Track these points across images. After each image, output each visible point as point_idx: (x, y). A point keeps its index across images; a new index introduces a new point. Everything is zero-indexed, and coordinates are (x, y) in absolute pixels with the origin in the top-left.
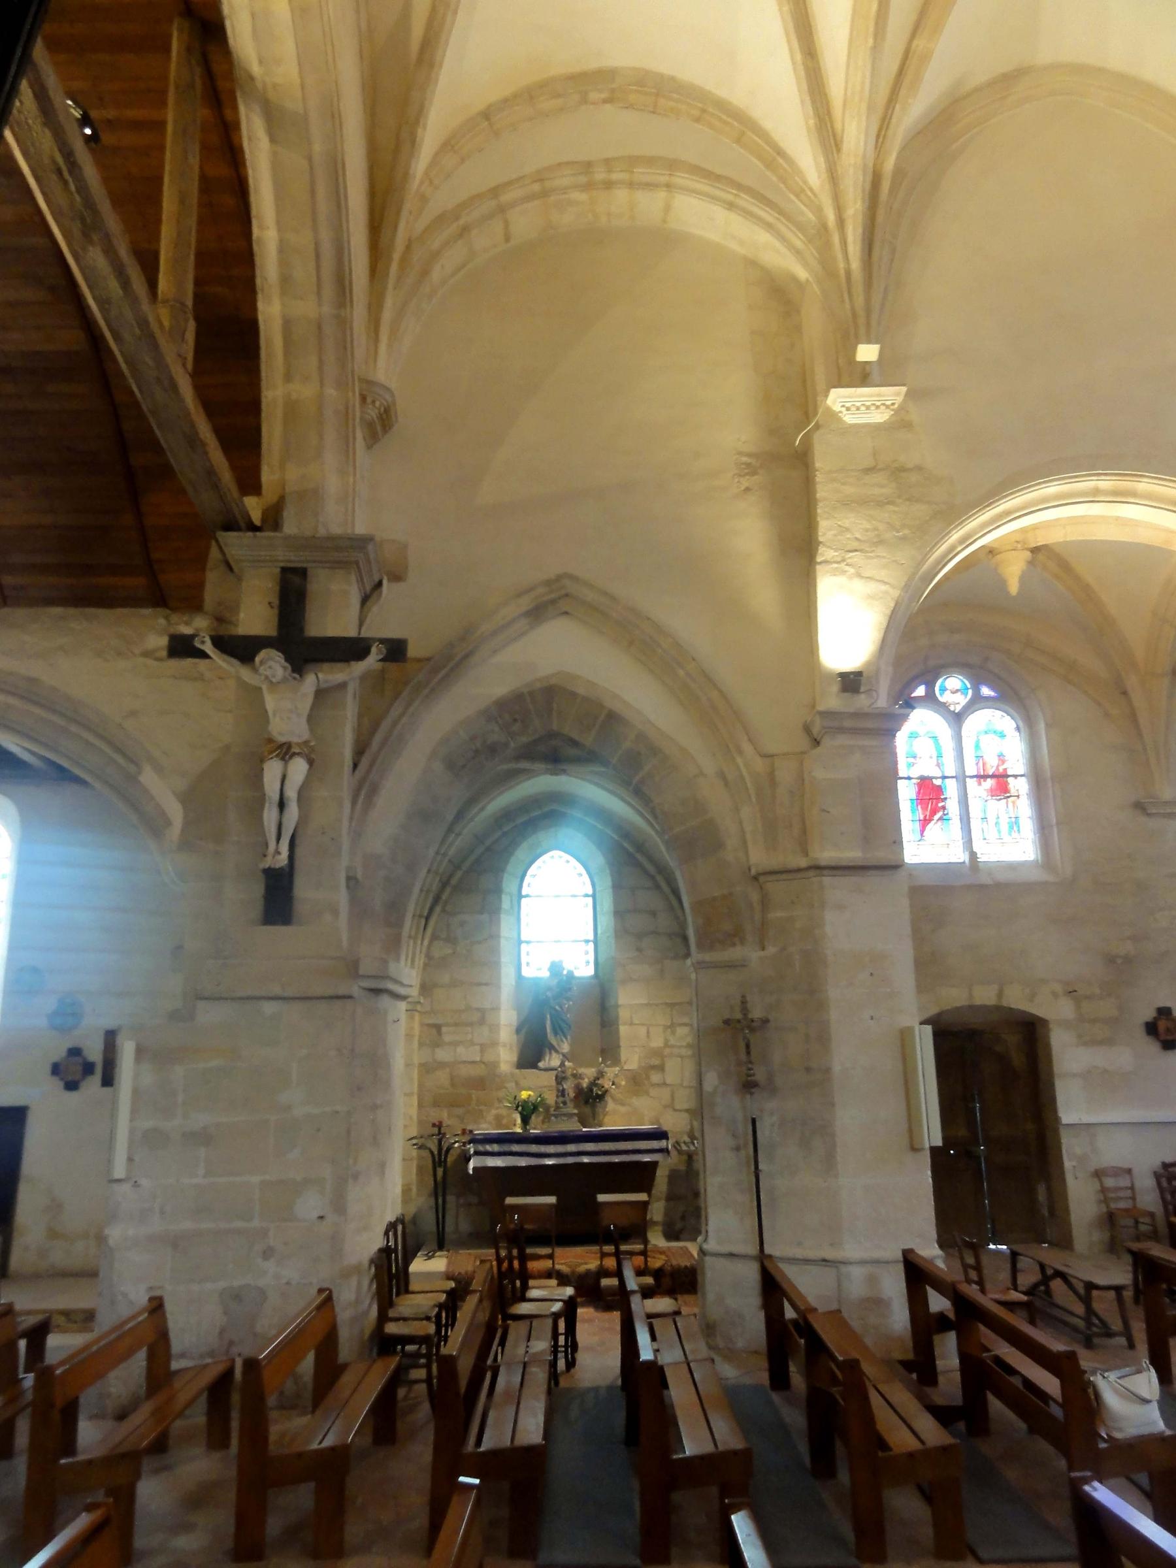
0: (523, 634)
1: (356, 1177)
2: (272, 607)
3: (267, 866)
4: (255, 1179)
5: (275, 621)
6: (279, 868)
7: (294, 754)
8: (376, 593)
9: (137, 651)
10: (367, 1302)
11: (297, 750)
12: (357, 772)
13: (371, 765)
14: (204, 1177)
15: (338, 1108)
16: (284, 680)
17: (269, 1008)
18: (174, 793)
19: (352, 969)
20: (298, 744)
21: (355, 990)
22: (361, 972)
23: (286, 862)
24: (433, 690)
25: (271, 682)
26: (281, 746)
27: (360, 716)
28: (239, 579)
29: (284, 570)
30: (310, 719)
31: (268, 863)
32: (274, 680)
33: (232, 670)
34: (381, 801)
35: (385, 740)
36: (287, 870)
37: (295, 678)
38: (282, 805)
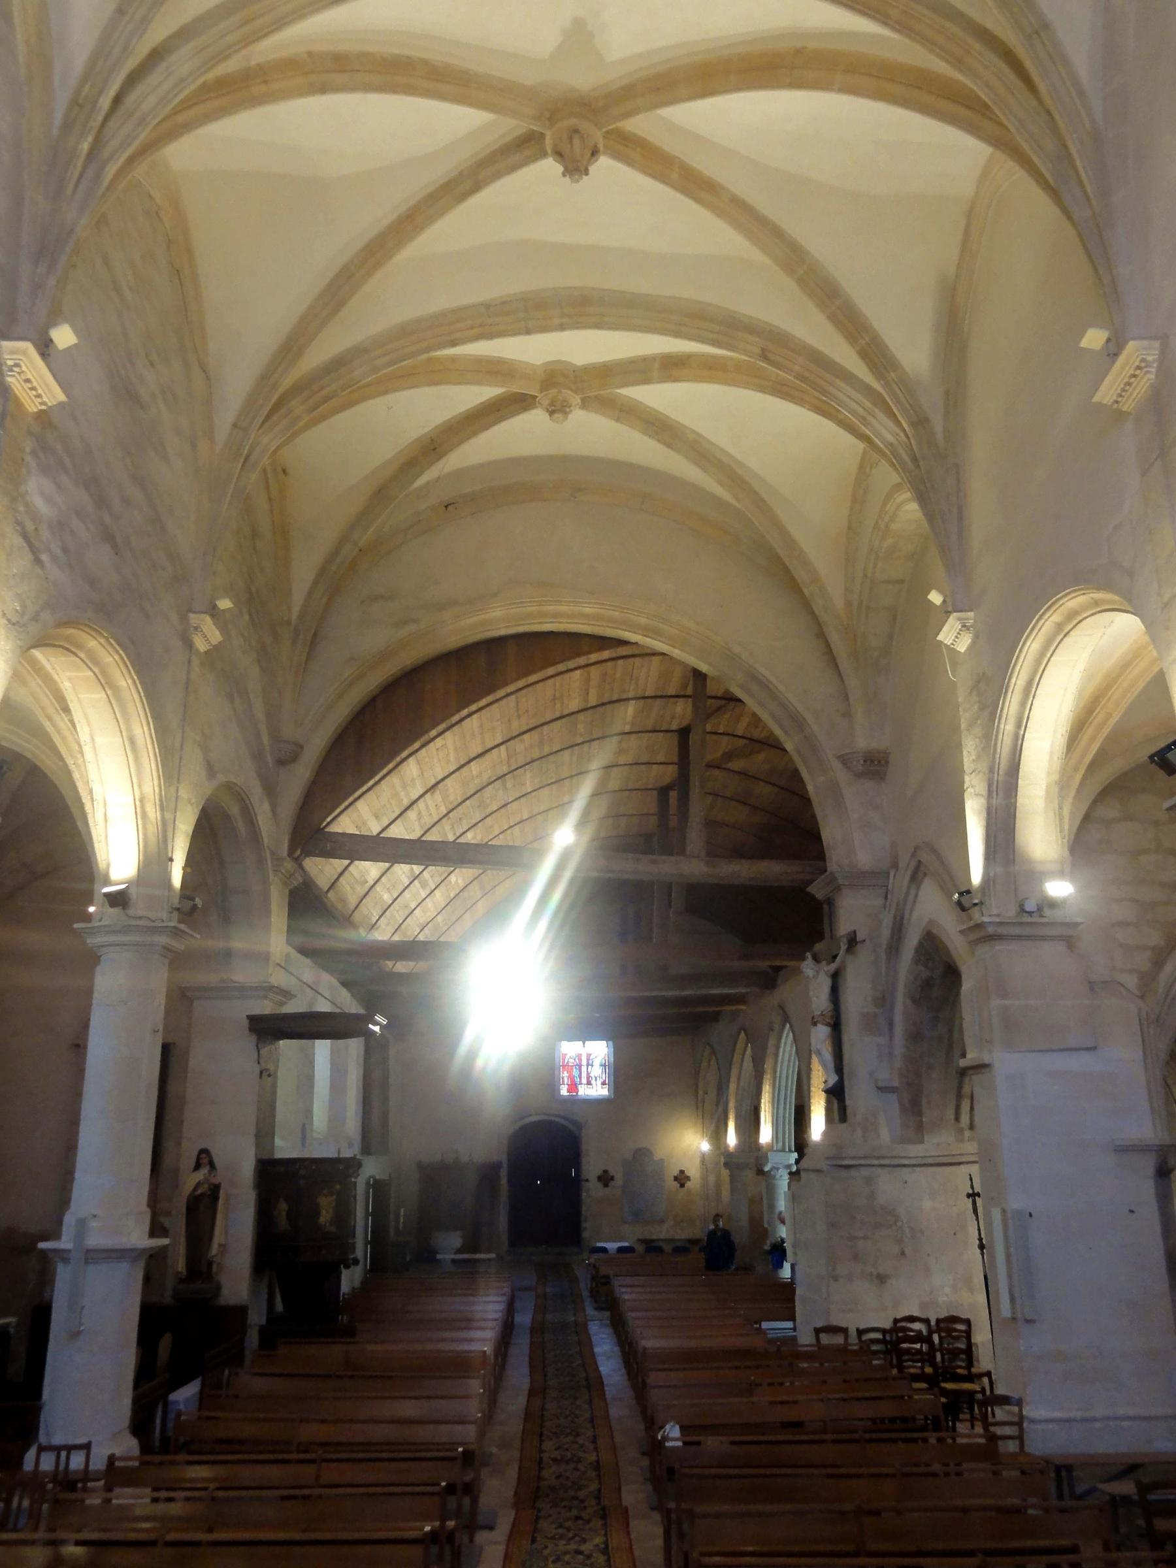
0: (916, 895)
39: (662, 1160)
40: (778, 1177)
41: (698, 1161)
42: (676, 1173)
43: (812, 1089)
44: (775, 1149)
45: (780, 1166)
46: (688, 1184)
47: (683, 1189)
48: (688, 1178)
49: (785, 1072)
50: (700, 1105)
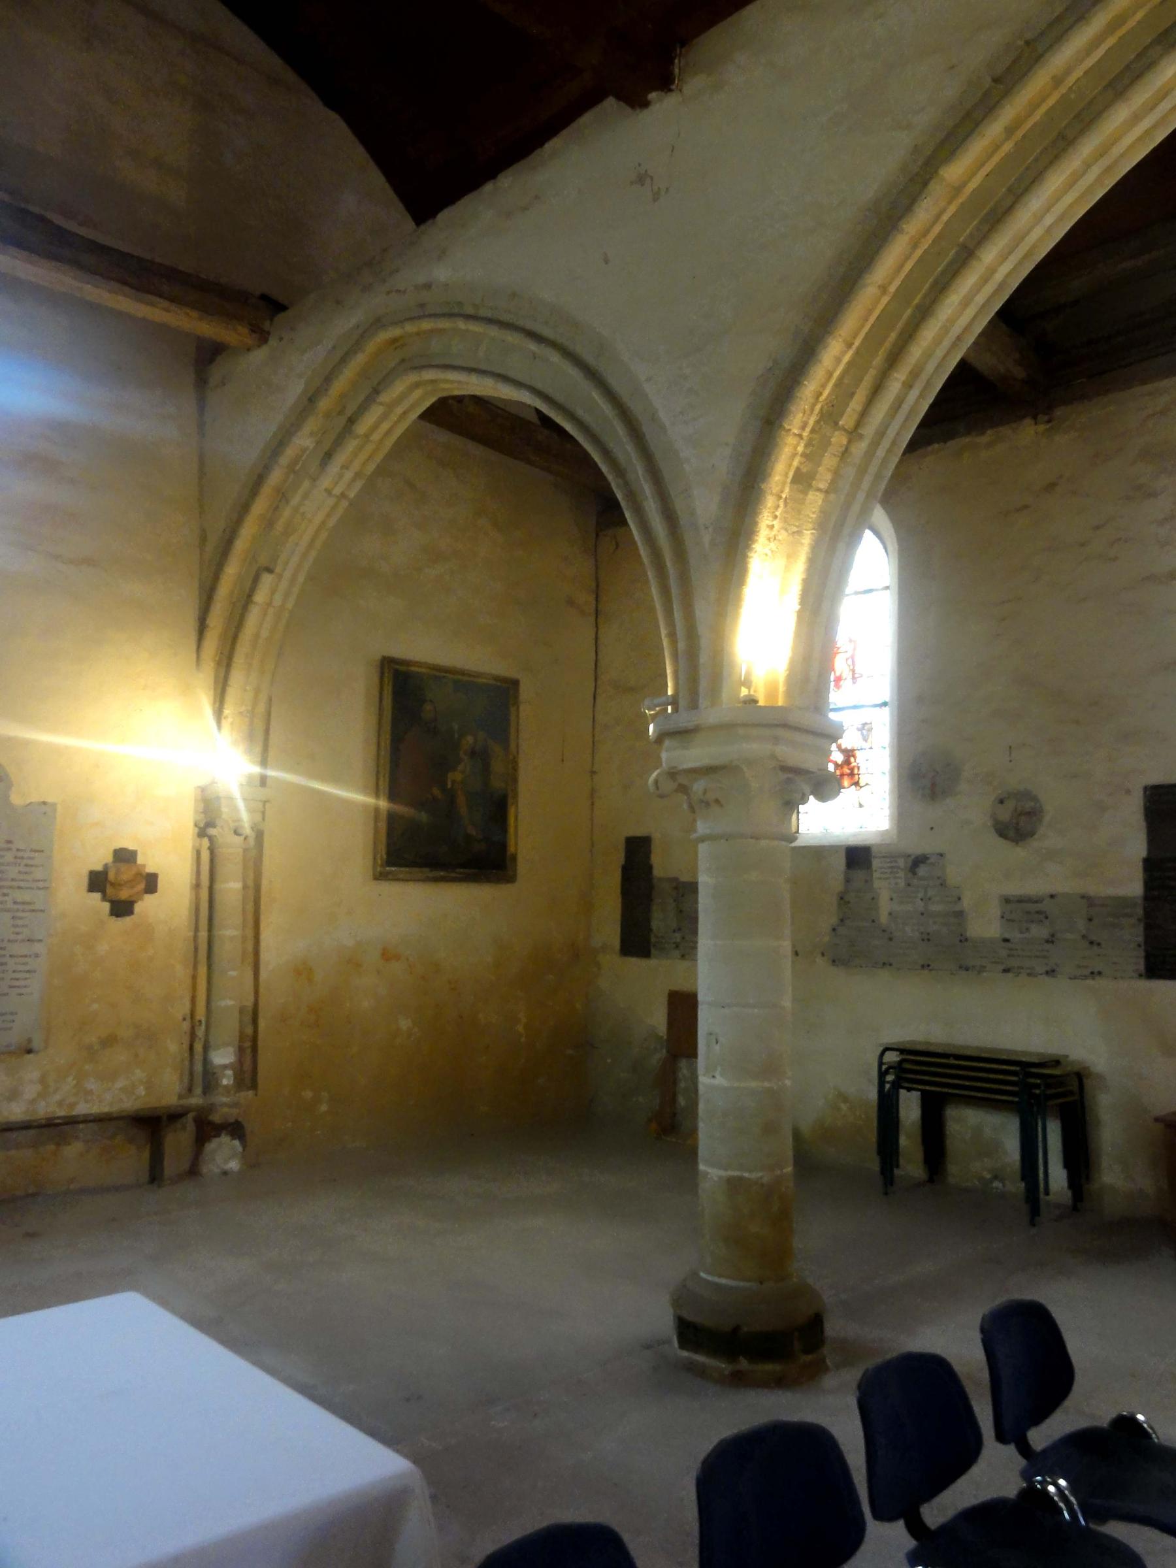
39: (45, 809)
41: (186, 818)
42: (99, 858)
46: (146, 906)
47: (127, 920)
48: (151, 883)
50: (216, 620)
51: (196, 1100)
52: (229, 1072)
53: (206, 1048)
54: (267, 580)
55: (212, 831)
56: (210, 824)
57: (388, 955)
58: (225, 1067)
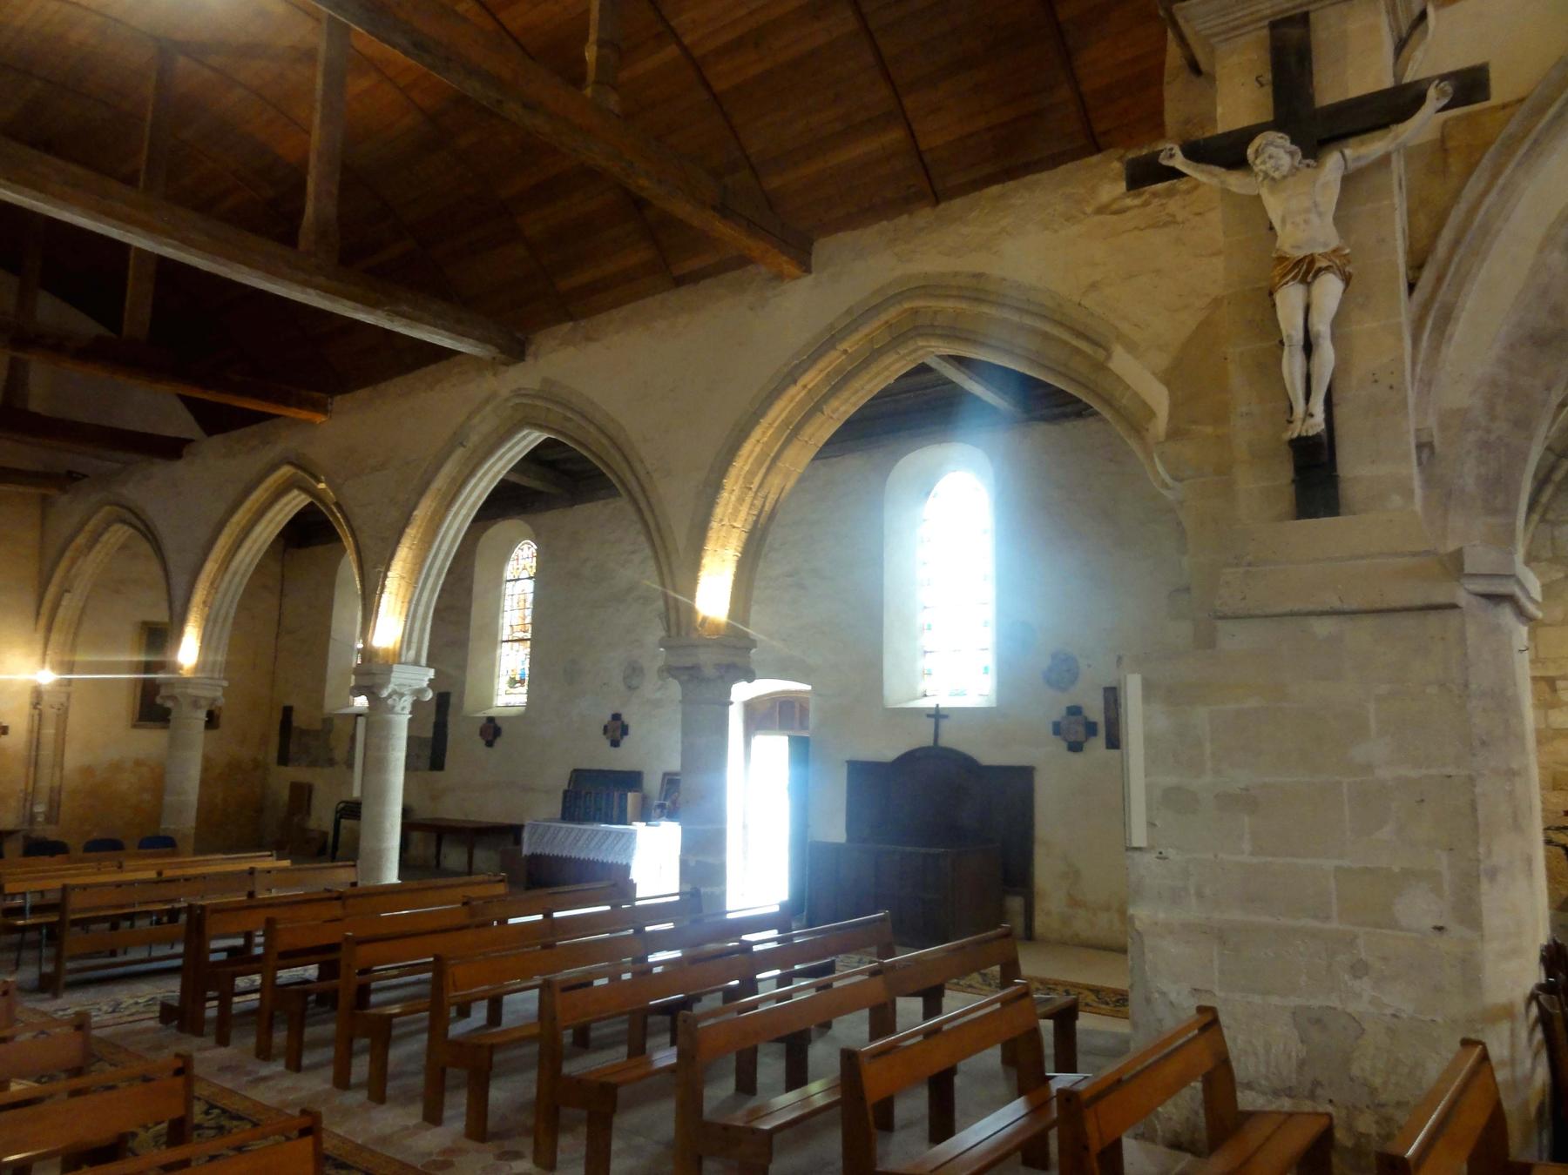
1: (1493, 874)
2: (1262, 85)
3: (1295, 435)
4: (1329, 864)
5: (1269, 102)
6: (1314, 437)
7: (1320, 270)
8: (1421, 28)
9: (1089, 210)
10: (1528, 1064)
11: (1323, 263)
12: (1416, 295)
13: (1439, 279)
14: (1252, 854)
15: (1450, 770)
16: (1294, 170)
17: (1323, 627)
18: (1154, 374)
19: (1454, 566)
20: (1324, 255)
21: (1462, 598)
22: (1468, 569)
23: (1323, 426)
24: (1536, 142)
25: (1273, 179)
26: (1301, 260)
27: (1411, 213)
28: (1212, 79)
29: (1274, 26)
30: (1337, 220)
31: (1297, 430)
32: (1277, 175)
33: (1215, 181)
34: (1460, 330)
35: (1457, 242)
36: (1325, 436)
37: (1308, 166)
38: (1309, 347)
40: (398, 709)
41: (26, 701)
43: (714, 525)
44: (403, 659)
45: (405, 690)
49: (455, 526)
50: (45, 609)
51: (26, 826)
52: (43, 815)
53: (32, 805)
54: (67, 596)
55: (39, 707)
56: (38, 703)
57: (138, 763)
58: (41, 813)
